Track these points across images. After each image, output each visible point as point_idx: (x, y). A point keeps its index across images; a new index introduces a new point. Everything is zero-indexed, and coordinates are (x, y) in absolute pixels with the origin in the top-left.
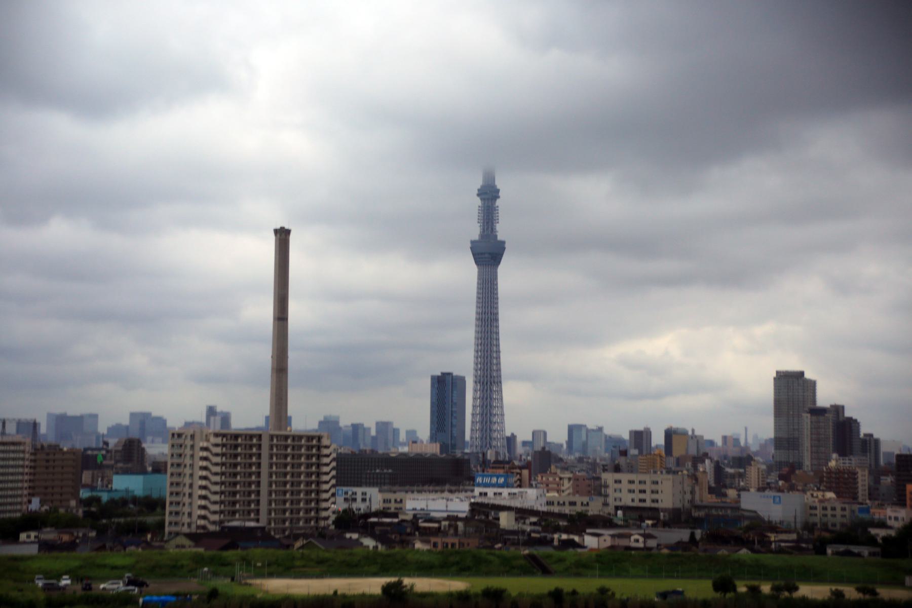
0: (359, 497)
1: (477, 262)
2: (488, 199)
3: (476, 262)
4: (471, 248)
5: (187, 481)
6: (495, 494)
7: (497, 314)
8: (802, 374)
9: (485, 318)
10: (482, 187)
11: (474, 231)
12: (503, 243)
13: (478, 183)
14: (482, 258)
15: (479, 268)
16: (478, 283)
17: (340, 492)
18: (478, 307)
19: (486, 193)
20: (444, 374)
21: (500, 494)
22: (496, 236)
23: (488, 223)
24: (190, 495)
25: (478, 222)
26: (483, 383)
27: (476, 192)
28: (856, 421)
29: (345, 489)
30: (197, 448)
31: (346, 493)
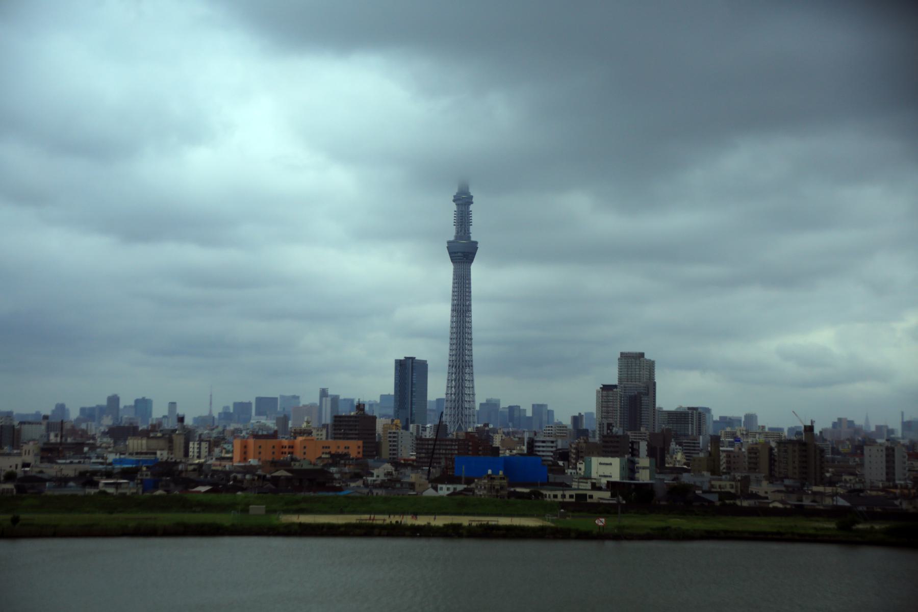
1: (453, 260)
2: (462, 204)
3: (452, 260)
4: (447, 247)
7: (470, 305)
9: (458, 309)
10: (457, 194)
12: (476, 243)
14: (456, 256)
15: (454, 266)
19: (459, 200)
20: (407, 358)
22: (469, 237)
23: (461, 225)
25: (454, 225)
27: (453, 198)
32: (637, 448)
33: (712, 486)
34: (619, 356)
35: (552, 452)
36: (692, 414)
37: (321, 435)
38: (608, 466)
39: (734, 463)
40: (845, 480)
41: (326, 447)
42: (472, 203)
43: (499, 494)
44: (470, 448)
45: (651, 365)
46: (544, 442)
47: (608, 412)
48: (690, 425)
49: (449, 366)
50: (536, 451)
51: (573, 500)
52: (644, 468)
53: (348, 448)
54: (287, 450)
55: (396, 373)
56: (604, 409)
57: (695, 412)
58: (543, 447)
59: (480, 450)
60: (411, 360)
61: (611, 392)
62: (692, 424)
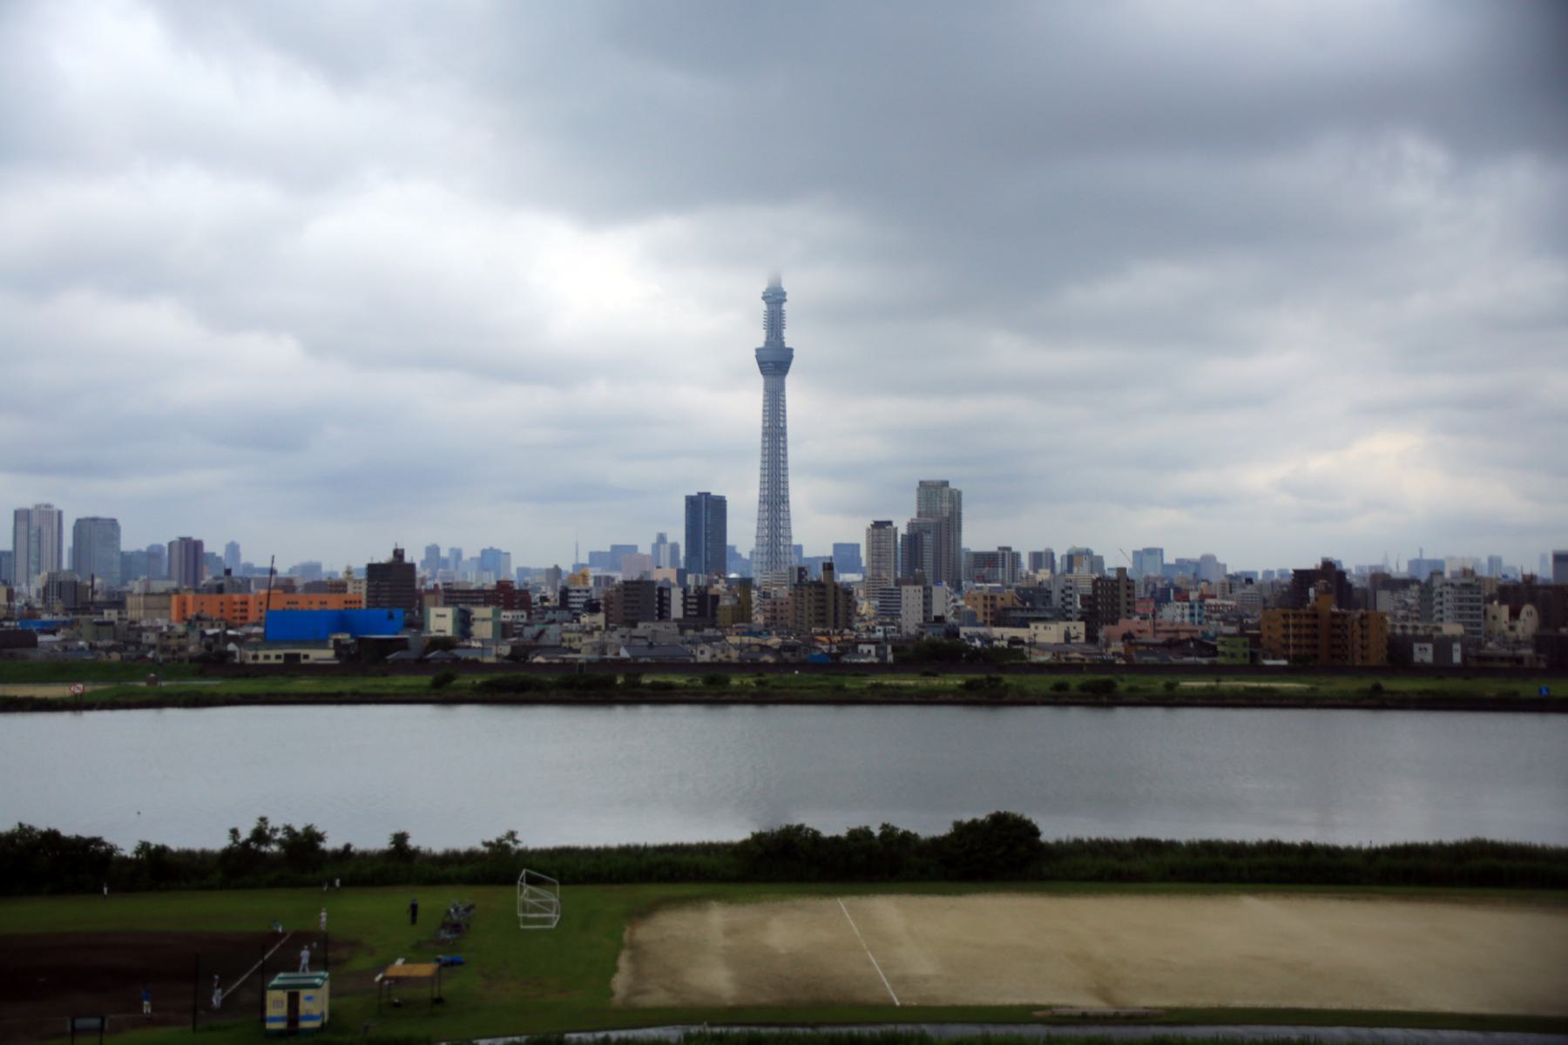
1: (763, 371)
2: (773, 303)
11: (760, 339)
13: (762, 287)
15: (765, 379)
20: (700, 494)
23: (772, 328)
26: (772, 503)
27: (762, 295)
32: (668, 596)
33: (563, 640)
34: (918, 485)
35: (582, 603)
36: (1003, 555)
37: (360, 588)
38: (443, 619)
39: (782, 611)
40: (858, 628)
41: (293, 603)
42: (785, 300)
43: (176, 657)
44: (501, 601)
45: (956, 499)
46: (578, 591)
47: (879, 555)
48: (1000, 569)
49: (760, 502)
50: (571, 603)
51: (281, 661)
52: (484, 620)
53: (325, 603)
54: (238, 607)
55: (687, 512)
56: (875, 550)
57: (1006, 552)
58: (578, 597)
59: (516, 604)
60: (704, 497)
61: (883, 530)
62: (1003, 566)
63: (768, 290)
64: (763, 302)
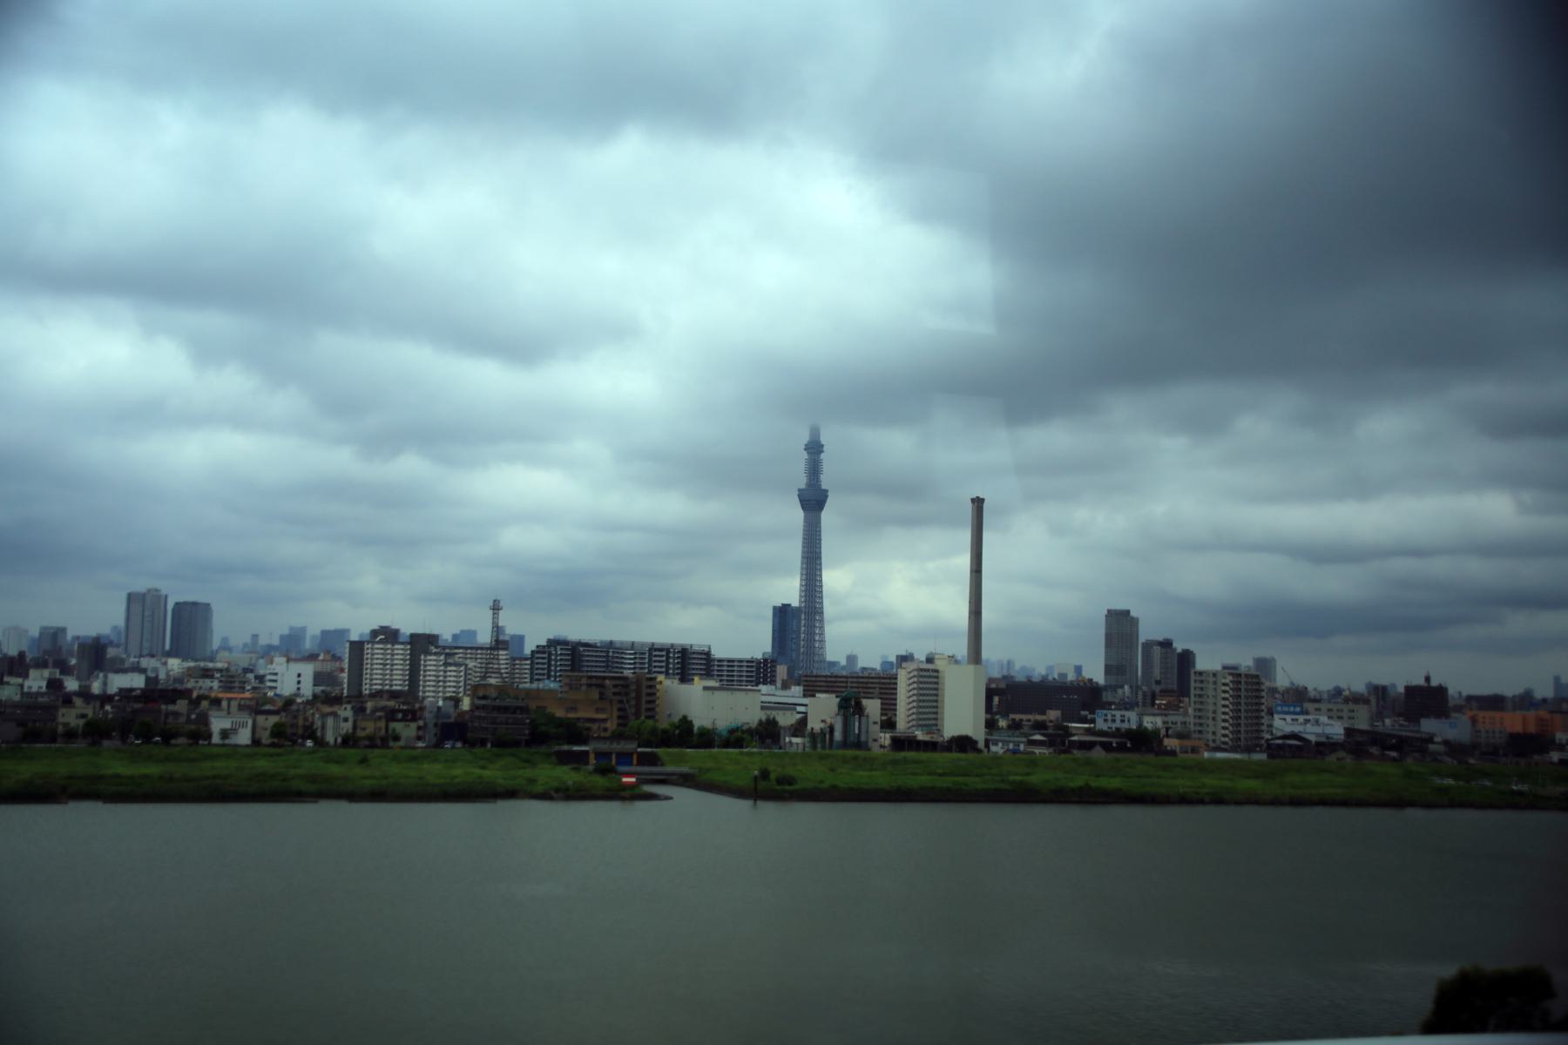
0: (1118, 718)
1: (803, 508)
5: (1211, 708)
6: (1293, 720)
7: (820, 553)
8: (1128, 612)
11: (802, 482)
13: (805, 438)
16: (804, 526)
17: (1100, 715)
18: (803, 547)
21: (1297, 720)
24: (1214, 719)
27: (803, 447)
28: (1192, 652)
29: (1105, 712)
30: (1219, 684)
31: (1106, 715)
42: (823, 452)
63: (809, 443)
64: (805, 453)
